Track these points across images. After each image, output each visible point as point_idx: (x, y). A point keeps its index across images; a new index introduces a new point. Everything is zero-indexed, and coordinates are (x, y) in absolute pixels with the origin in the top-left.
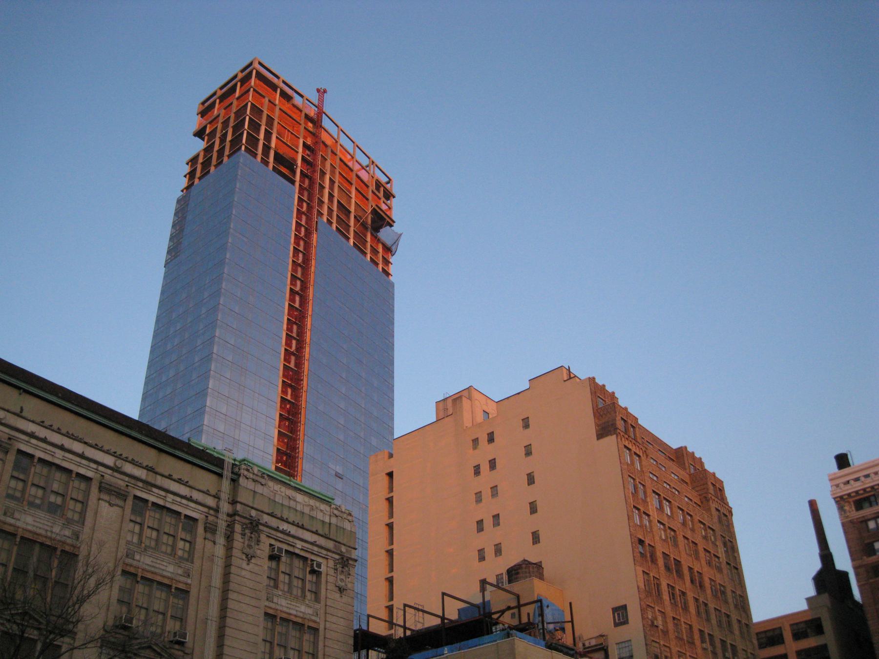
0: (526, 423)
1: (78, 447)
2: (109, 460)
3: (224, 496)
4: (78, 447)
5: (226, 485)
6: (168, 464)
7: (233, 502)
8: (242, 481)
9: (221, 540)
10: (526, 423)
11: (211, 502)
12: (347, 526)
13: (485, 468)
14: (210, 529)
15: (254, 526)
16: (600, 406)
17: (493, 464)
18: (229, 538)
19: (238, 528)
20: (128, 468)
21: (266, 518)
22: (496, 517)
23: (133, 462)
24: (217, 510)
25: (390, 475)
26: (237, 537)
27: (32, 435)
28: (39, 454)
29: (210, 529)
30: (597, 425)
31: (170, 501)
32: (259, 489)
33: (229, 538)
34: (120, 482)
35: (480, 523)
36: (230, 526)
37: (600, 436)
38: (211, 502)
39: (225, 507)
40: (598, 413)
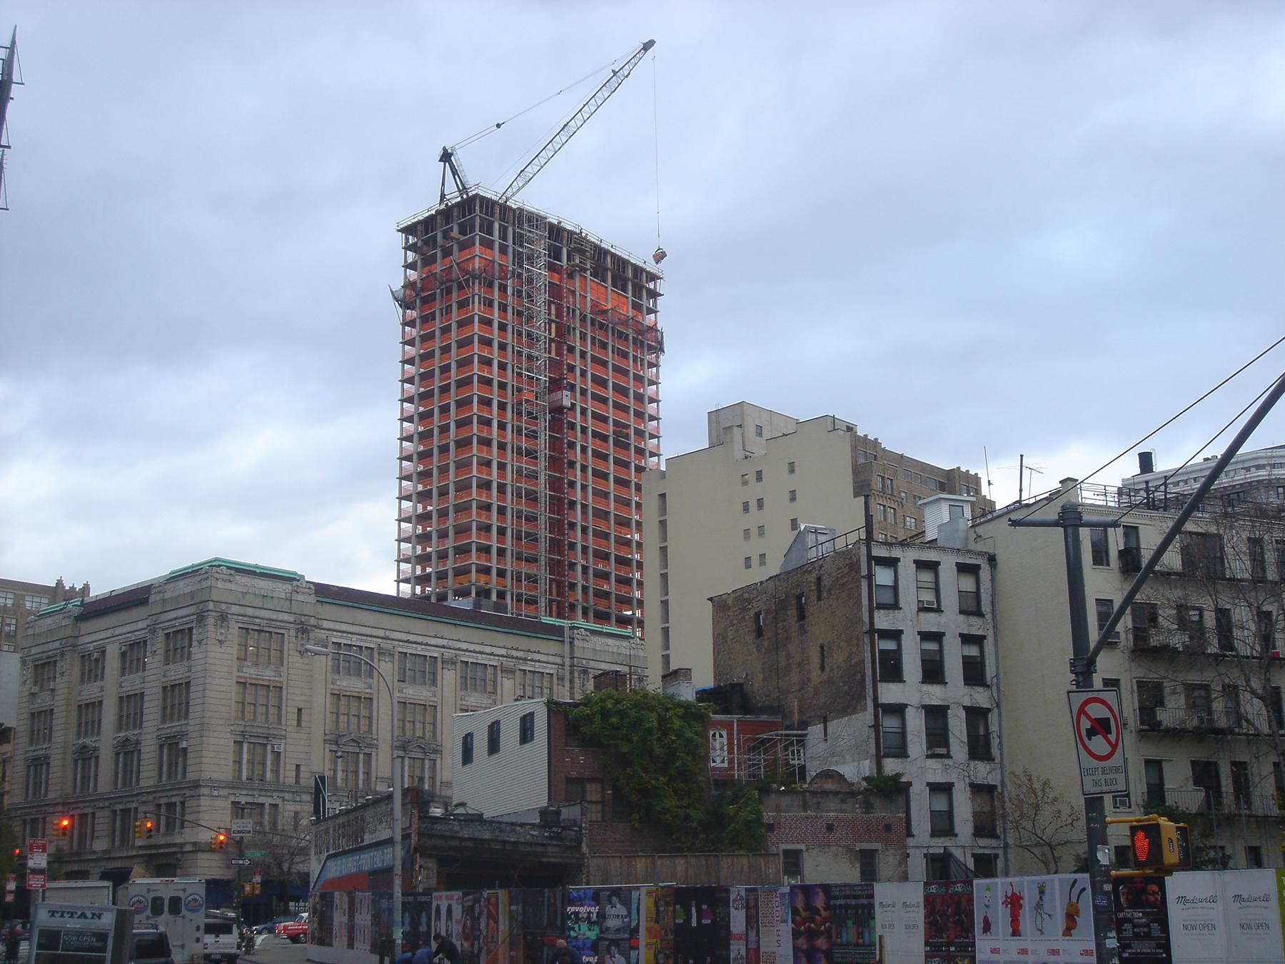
0: (792, 468)
1: (488, 649)
2: (503, 652)
3: (567, 655)
4: (488, 649)
5: (567, 646)
6: (534, 644)
7: (572, 658)
8: (576, 642)
9: (567, 684)
10: (792, 468)
11: (559, 660)
12: (642, 654)
13: (753, 505)
14: (561, 679)
15: (585, 671)
16: (862, 461)
17: (760, 504)
18: (572, 682)
19: (576, 674)
20: (515, 653)
21: (592, 664)
22: (763, 556)
23: (517, 649)
24: (563, 665)
25: (663, 496)
26: (576, 680)
27: (467, 650)
28: (470, 660)
29: (561, 679)
30: (854, 482)
31: (538, 667)
32: (586, 645)
33: (572, 682)
34: (509, 663)
35: (748, 559)
36: (572, 673)
37: (856, 495)
38: (559, 660)
39: (568, 662)
40: (856, 470)
